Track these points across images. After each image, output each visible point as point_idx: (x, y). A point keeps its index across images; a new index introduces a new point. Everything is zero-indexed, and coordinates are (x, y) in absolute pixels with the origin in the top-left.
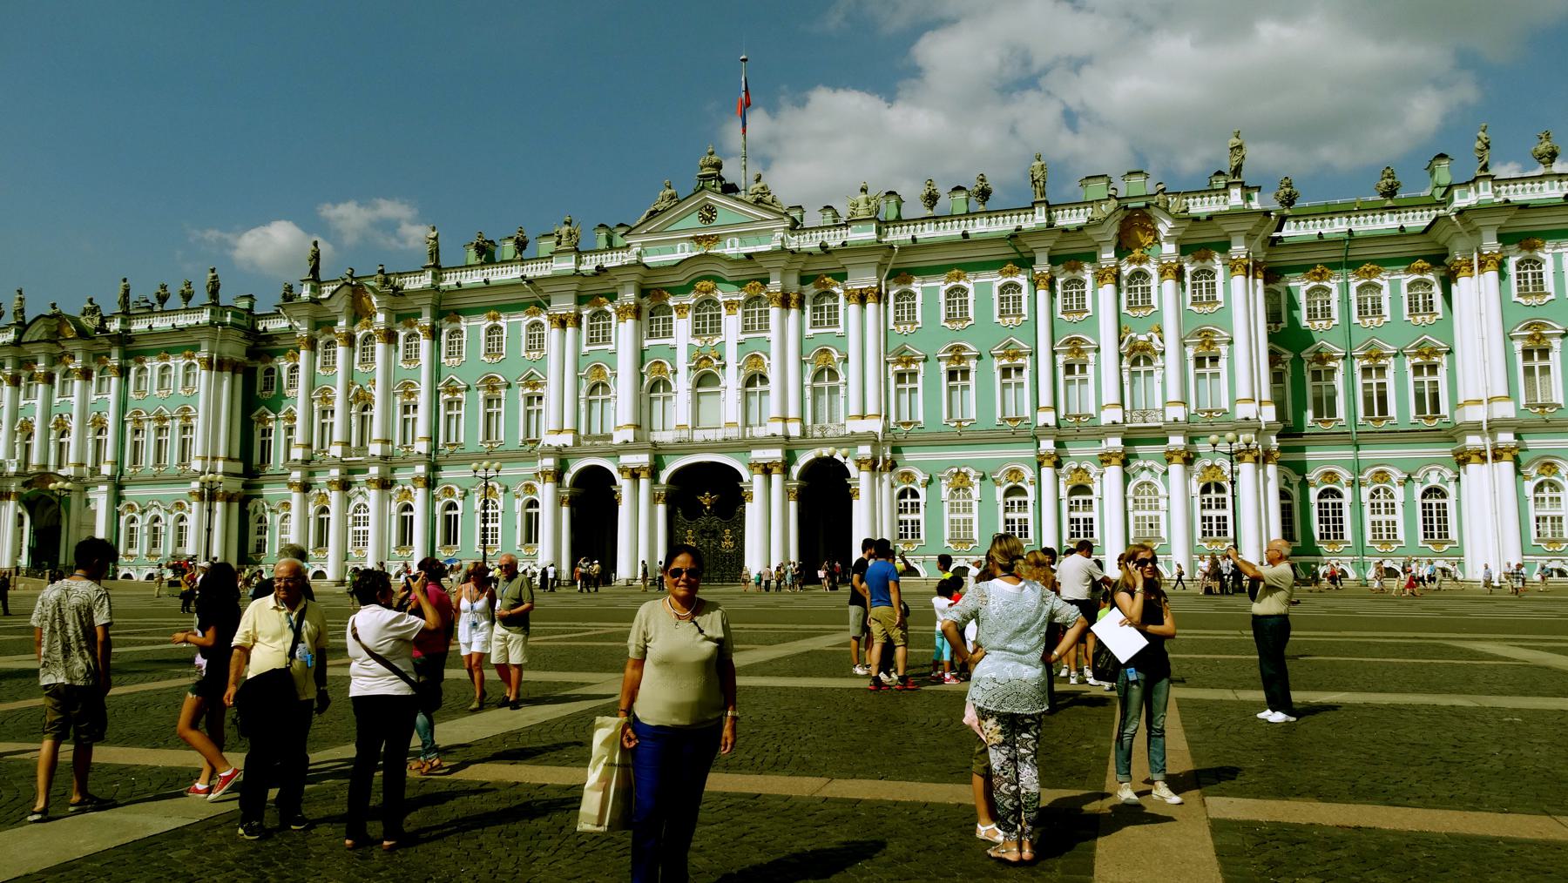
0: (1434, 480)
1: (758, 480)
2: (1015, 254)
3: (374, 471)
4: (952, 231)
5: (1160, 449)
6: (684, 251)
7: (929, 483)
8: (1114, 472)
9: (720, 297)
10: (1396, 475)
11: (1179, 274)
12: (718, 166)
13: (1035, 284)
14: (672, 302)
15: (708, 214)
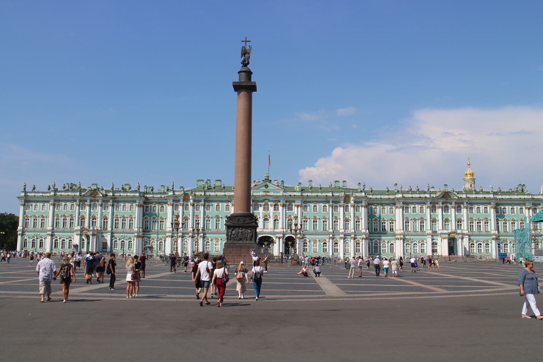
0: (392, 242)
1: (277, 240)
2: (326, 200)
3: (191, 234)
4: (315, 194)
5: (350, 237)
6: (261, 194)
7: (310, 241)
8: (342, 241)
9: (269, 203)
10: (386, 241)
11: (354, 207)
12: (268, 177)
13: (329, 206)
14: (259, 203)
15: (266, 186)
